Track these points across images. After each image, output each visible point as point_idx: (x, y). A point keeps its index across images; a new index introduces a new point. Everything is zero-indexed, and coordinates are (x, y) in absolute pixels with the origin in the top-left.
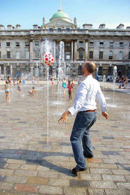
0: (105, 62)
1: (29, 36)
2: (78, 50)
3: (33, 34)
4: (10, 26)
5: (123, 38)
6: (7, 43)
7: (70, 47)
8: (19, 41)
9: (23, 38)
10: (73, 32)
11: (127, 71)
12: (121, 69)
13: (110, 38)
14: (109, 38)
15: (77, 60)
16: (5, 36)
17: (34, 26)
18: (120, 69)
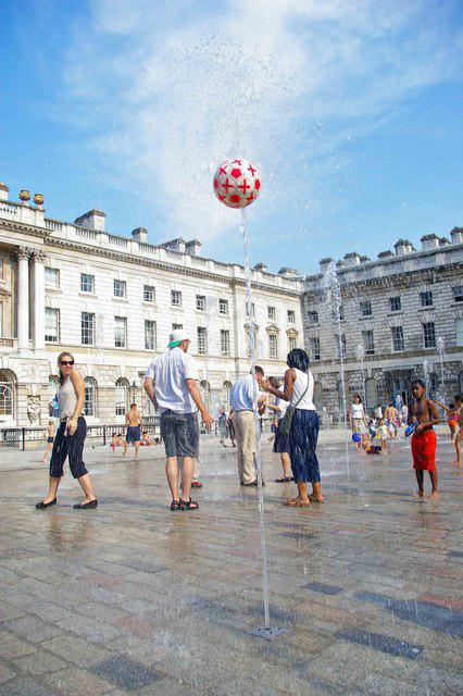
4: (432, 237)
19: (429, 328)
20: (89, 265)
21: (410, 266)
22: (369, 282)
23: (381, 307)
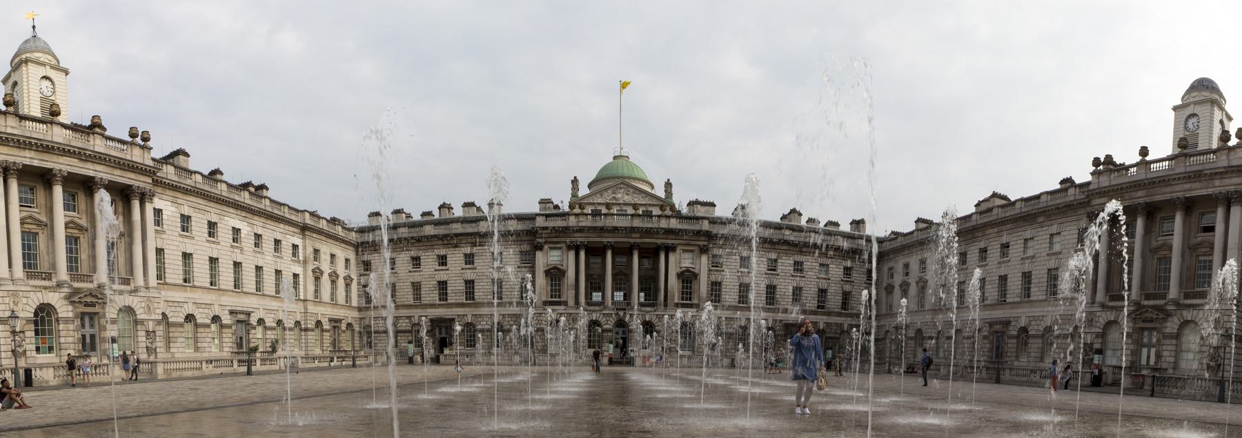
1: (533, 233)
2: (680, 275)
6: (466, 255)
7: (656, 269)
10: (664, 224)
15: (677, 305)
16: (461, 235)
19: (470, 284)
20: (188, 205)
21: (457, 228)
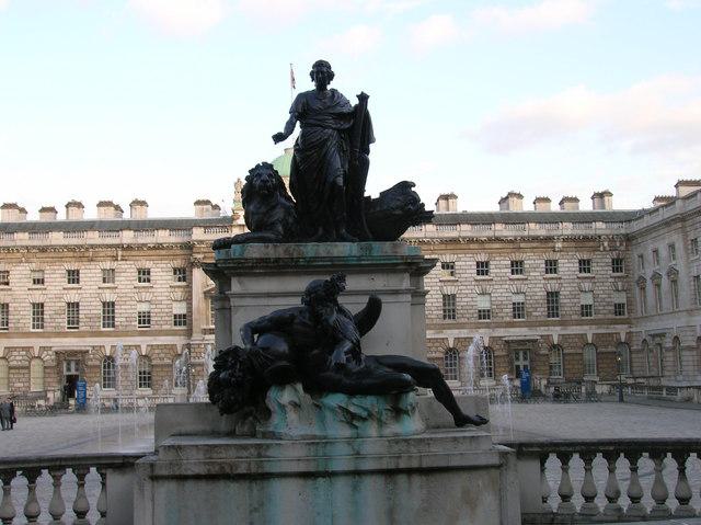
0: (465, 331)
3: (201, 242)
4: (109, 204)
5: (522, 245)
8: (148, 265)
9: (163, 252)
11: (544, 359)
12: (525, 353)
13: (476, 246)
14: (472, 246)
17: (198, 203)
18: (521, 354)
19: (109, 307)
21: (93, 238)
22: (43, 249)
23: (56, 277)
